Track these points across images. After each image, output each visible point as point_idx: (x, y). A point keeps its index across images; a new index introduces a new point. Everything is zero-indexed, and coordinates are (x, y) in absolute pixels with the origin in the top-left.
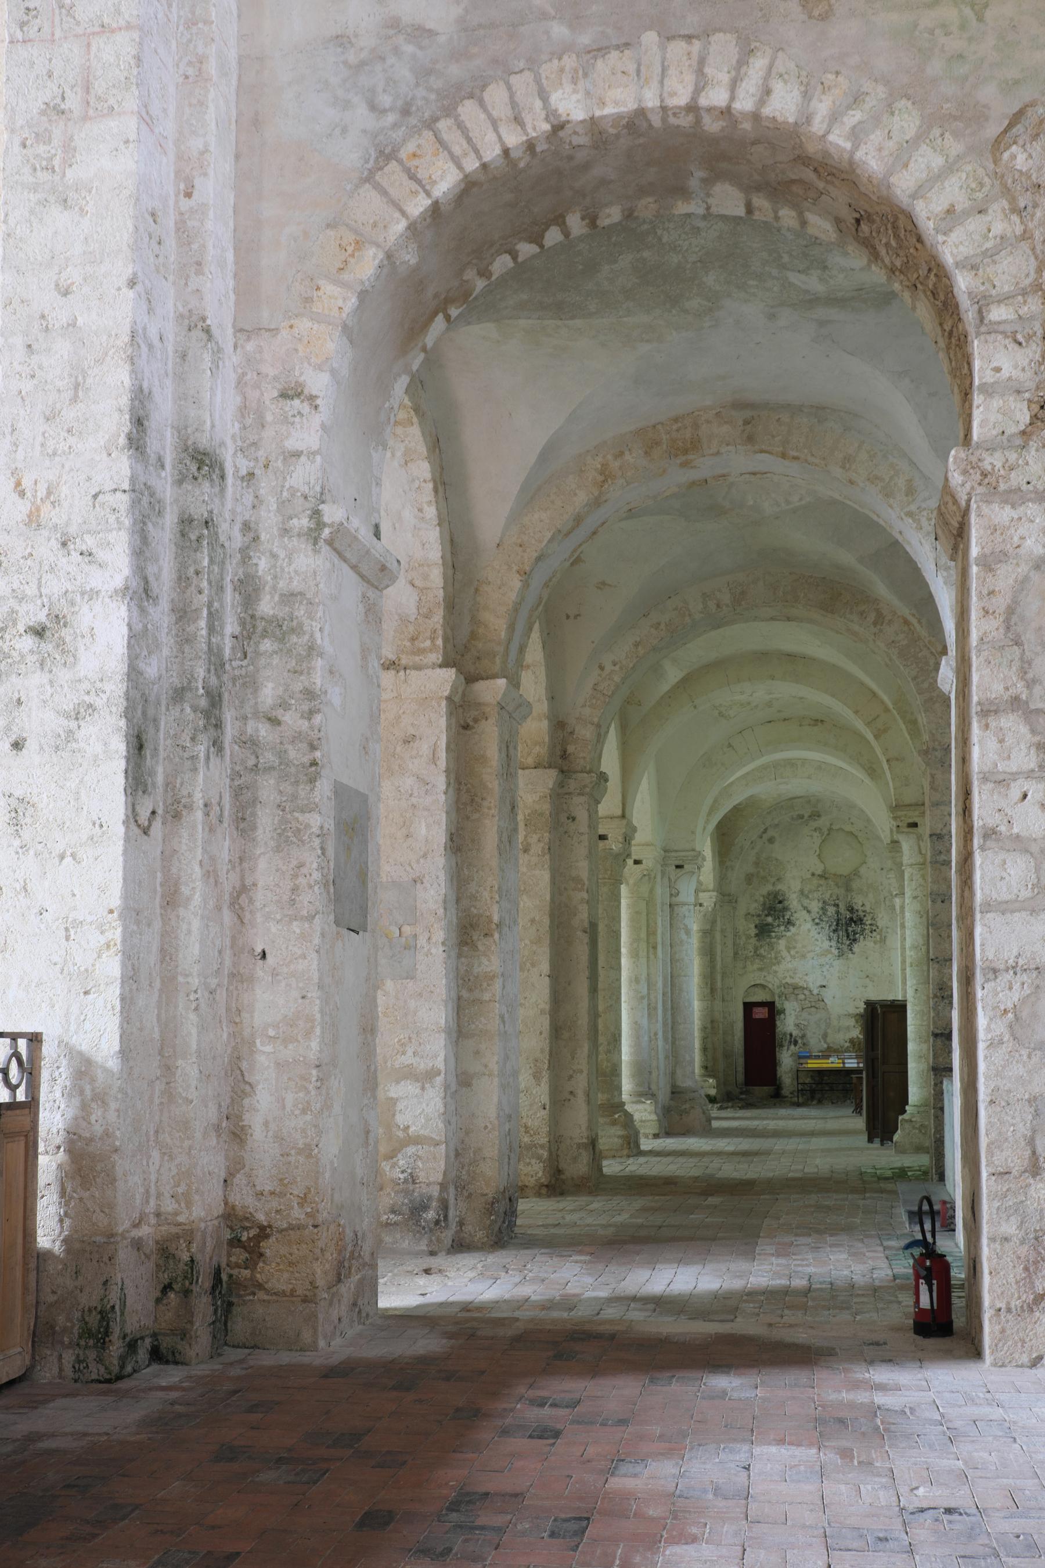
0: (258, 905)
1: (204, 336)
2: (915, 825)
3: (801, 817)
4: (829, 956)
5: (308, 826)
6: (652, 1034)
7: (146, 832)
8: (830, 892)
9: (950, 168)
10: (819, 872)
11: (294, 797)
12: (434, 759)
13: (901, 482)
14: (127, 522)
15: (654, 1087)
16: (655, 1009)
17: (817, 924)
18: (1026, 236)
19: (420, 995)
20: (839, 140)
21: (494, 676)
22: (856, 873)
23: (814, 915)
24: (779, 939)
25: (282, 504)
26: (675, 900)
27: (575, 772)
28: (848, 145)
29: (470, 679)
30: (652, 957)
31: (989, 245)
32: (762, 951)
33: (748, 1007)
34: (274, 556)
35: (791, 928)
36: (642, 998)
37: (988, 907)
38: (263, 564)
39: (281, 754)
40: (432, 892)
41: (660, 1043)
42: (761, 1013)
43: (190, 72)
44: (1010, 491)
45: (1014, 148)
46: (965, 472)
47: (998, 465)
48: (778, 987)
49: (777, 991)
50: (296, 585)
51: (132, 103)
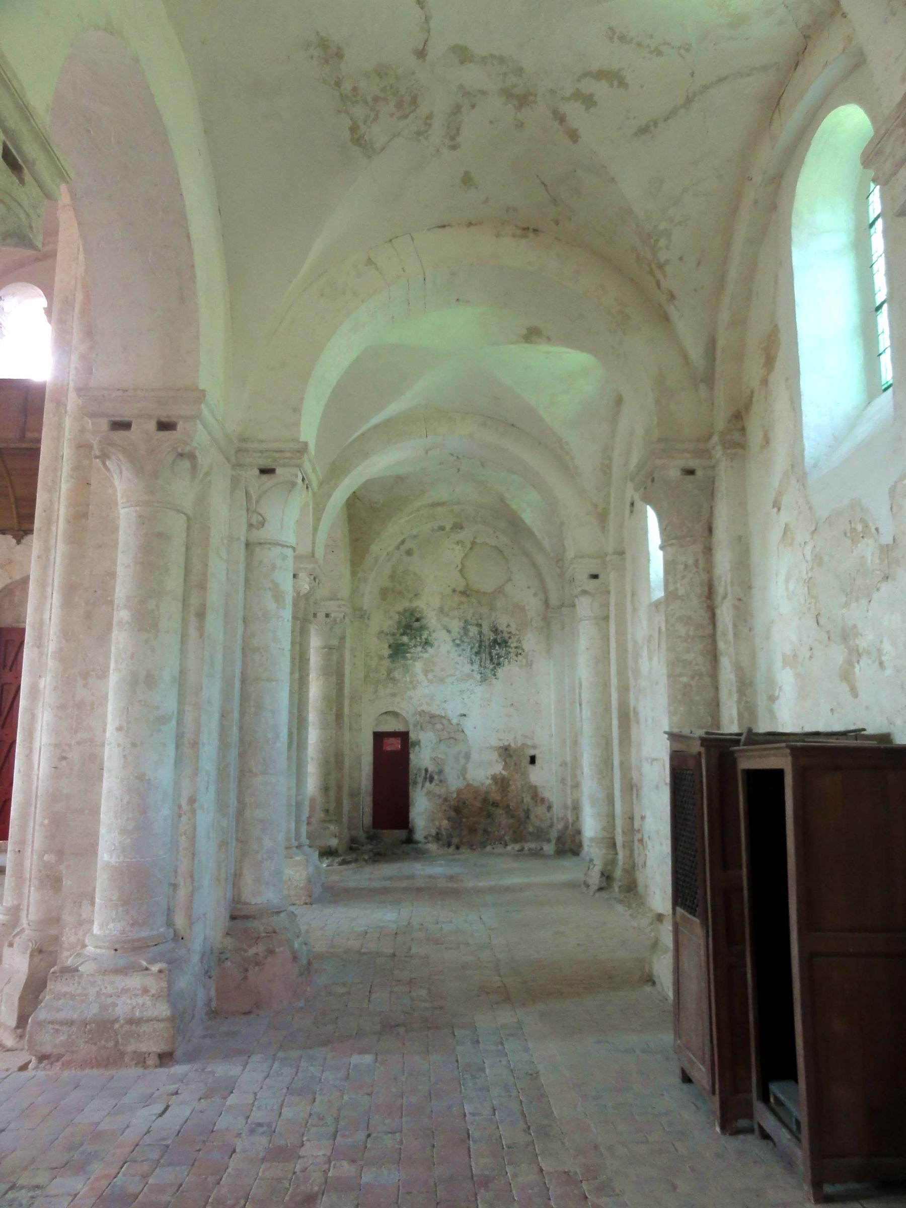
3: (442, 528)
4: (471, 681)
6: (184, 802)
8: (471, 611)
10: (461, 588)
15: (180, 920)
16: (195, 745)
17: (458, 645)
23: (455, 634)
24: (414, 661)
26: (257, 535)
30: (193, 633)
33: (379, 737)
36: (163, 720)
41: (205, 819)
42: (394, 745)
48: (414, 715)
49: (411, 721)
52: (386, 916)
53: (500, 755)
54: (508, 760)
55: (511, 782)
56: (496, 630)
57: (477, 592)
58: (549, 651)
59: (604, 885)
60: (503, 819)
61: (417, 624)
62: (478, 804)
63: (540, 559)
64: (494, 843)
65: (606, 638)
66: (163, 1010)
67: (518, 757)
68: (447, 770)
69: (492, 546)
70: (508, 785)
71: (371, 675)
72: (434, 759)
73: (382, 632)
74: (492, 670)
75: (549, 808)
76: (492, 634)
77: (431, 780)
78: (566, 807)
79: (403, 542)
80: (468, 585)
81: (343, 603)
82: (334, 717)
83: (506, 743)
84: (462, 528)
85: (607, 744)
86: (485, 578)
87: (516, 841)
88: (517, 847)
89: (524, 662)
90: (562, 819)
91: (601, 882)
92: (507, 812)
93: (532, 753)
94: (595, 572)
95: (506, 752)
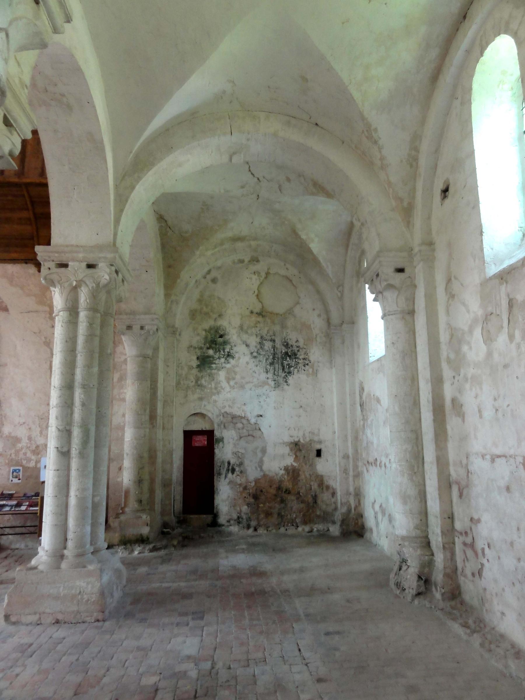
3: (242, 261)
4: (267, 387)
10: (257, 309)
17: (255, 357)
22: (290, 312)
23: (253, 348)
24: (219, 370)
32: (203, 382)
33: (188, 435)
35: (231, 360)
42: (201, 441)
48: (217, 416)
49: (216, 421)
53: (291, 450)
54: (298, 454)
55: (300, 473)
56: (287, 344)
57: (271, 313)
58: (331, 362)
59: (422, 589)
60: (294, 505)
61: (221, 340)
62: (273, 491)
63: (323, 286)
64: (287, 525)
65: (412, 332)
67: (306, 451)
68: (247, 462)
69: (283, 276)
70: (299, 475)
71: (182, 382)
72: (235, 454)
73: (191, 346)
74: (284, 378)
75: (334, 494)
76: (283, 348)
77: (233, 471)
78: (348, 494)
79: (209, 272)
80: (263, 307)
81: (157, 317)
82: (147, 418)
83: (296, 440)
84: (258, 261)
85: (417, 439)
86: (278, 301)
87: (305, 523)
88: (307, 528)
89: (311, 370)
90: (346, 503)
91: (419, 586)
92: (298, 499)
93: (318, 447)
94: (400, 266)
95: (296, 447)
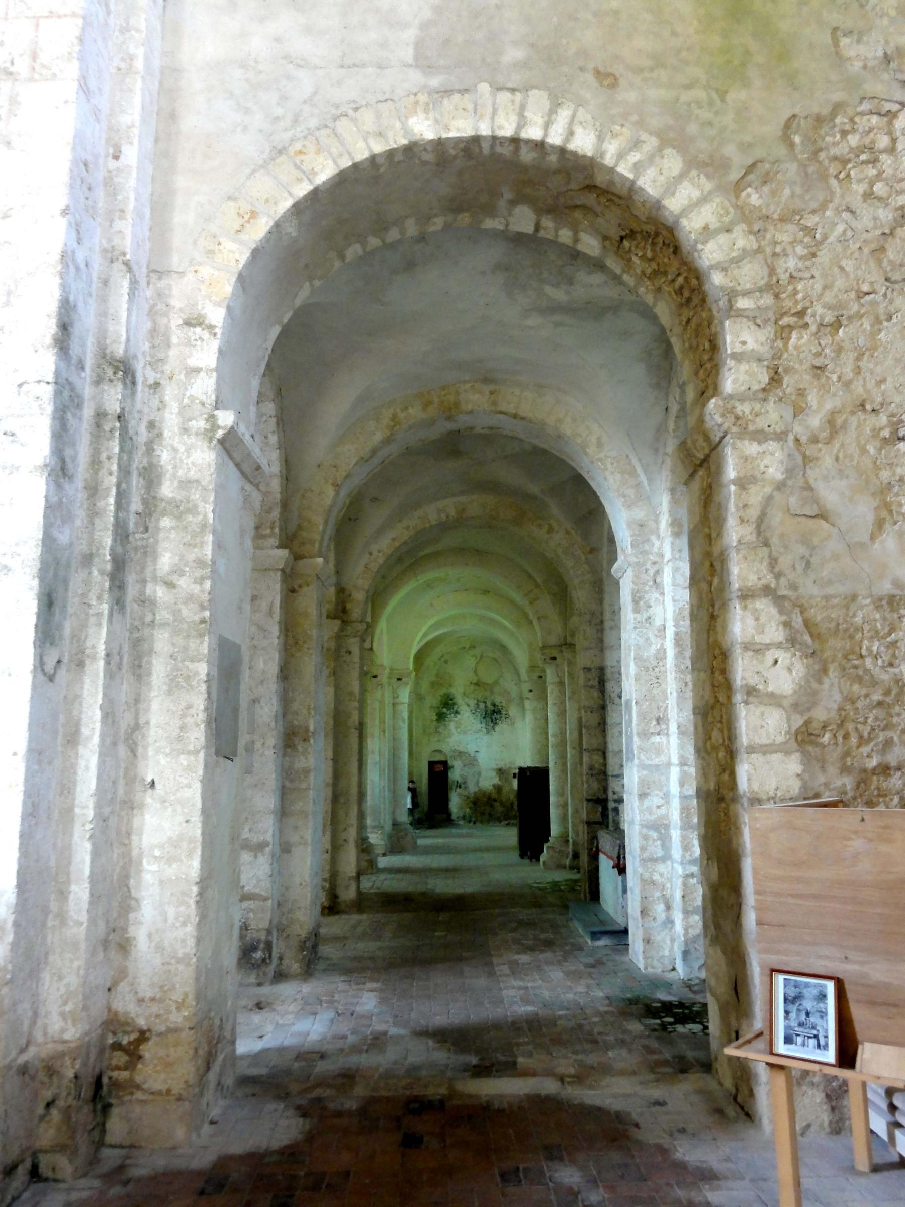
0: (150, 740)
1: (124, 268)
2: (554, 659)
5: (197, 674)
7: (51, 679)
9: (704, 200)
11: (186, 649)
12: (270, 613)
13: (593, 438)
14: (49, 409)
18: (759, 250)
19: (256, 786)
20: (624, 169)
21: (314, 557)
22: (496, 683)
25: (183, 409)
27: (353, 622)
28: (631, 176)
29: (298, 557)
31: (734, 254)
33: (432, 764)
34: (175, 450)
37: (751, 750)
38: (164, 456)
39: (176, 613)
40: (267, 710)
42: (440, 768)
43: (123, 65)
44: (757, 432)
45: (749, 190)
46: (723, 416)
47: (747, 412)
50: (193, 474)
51: (73, 70)
52: (440, 841)
66: (382, 843)
68: (469, 782)
72: (461, 776)
